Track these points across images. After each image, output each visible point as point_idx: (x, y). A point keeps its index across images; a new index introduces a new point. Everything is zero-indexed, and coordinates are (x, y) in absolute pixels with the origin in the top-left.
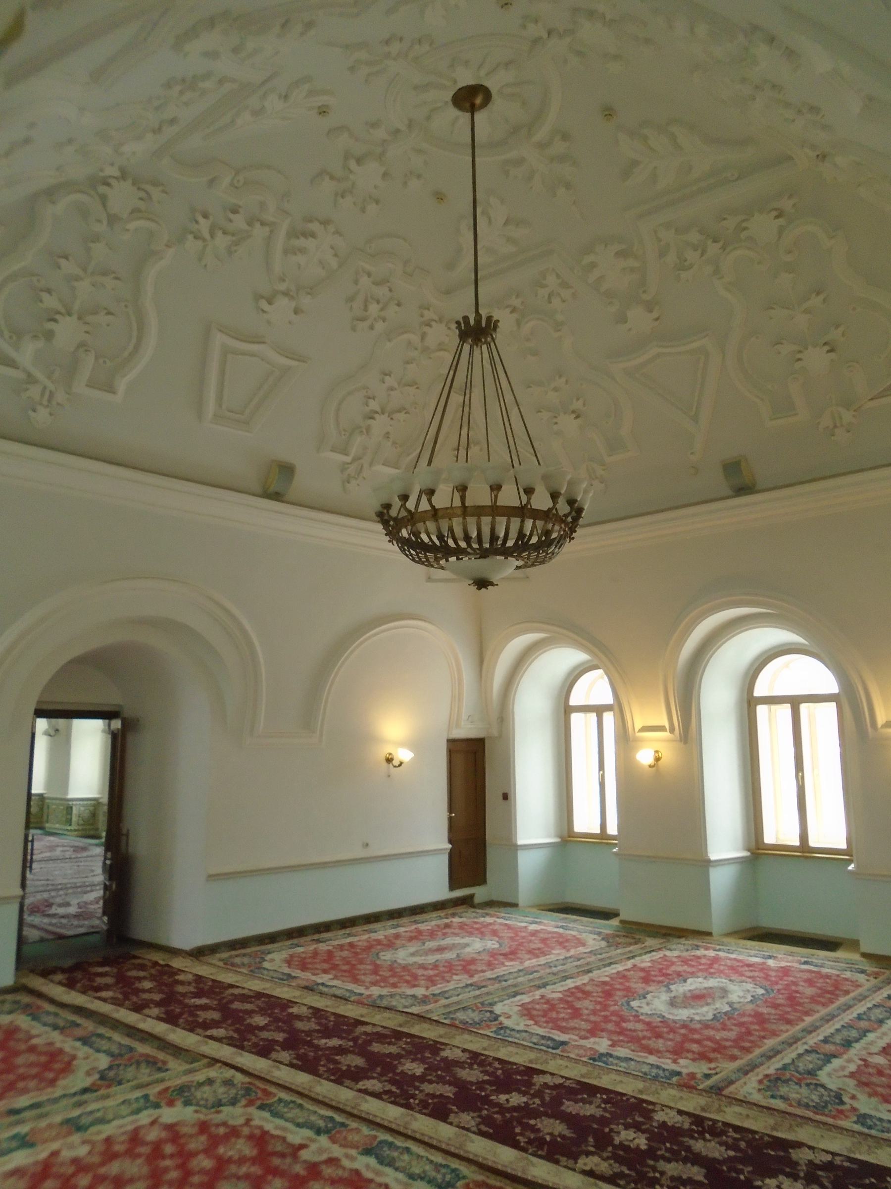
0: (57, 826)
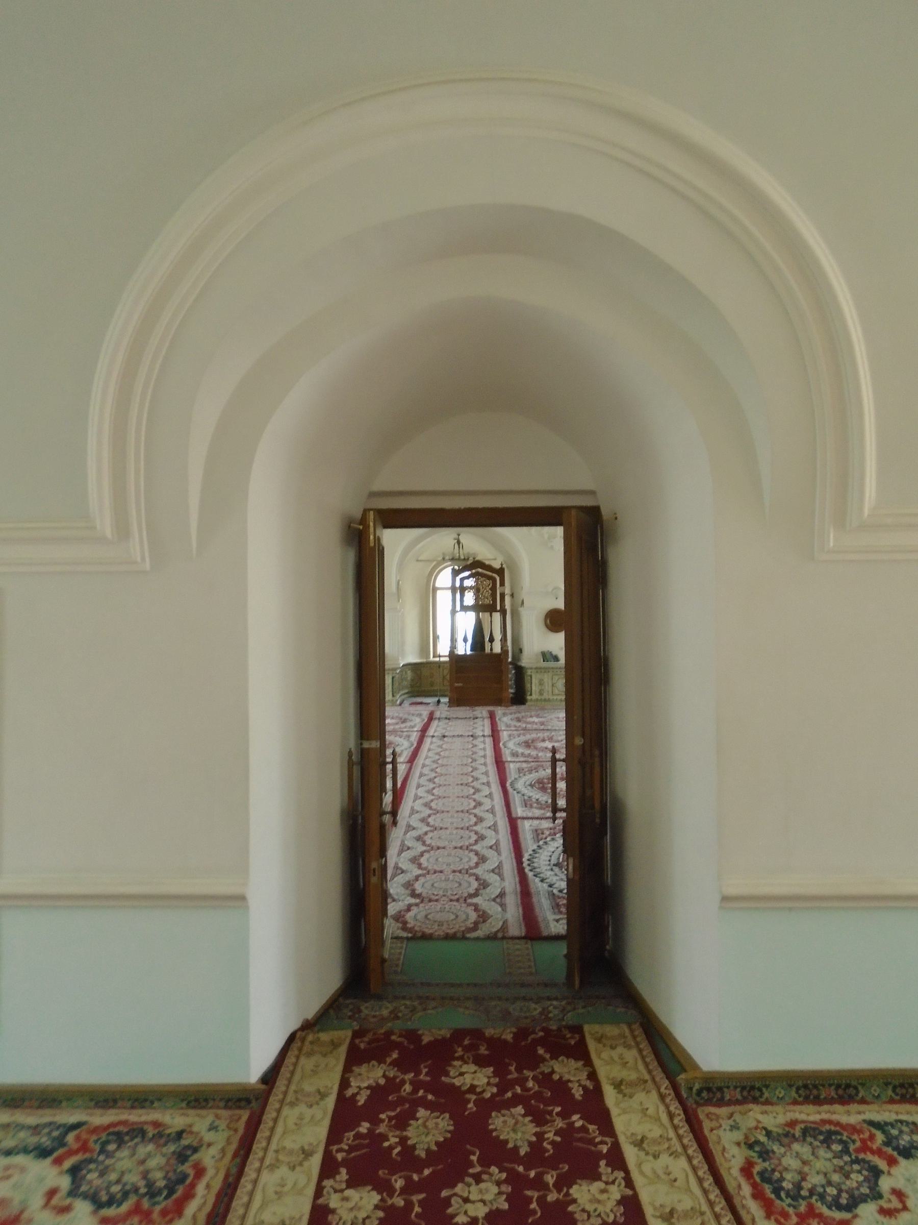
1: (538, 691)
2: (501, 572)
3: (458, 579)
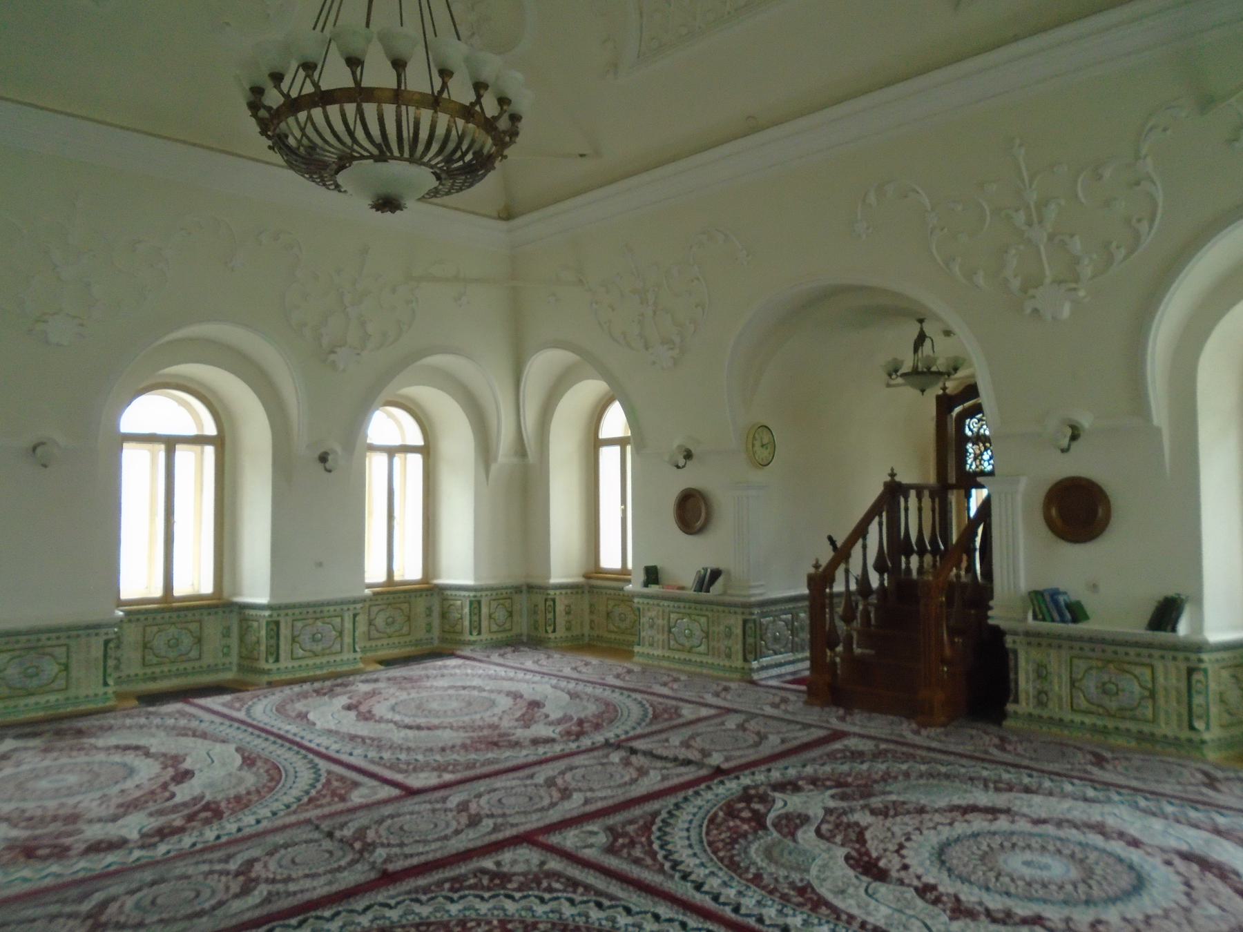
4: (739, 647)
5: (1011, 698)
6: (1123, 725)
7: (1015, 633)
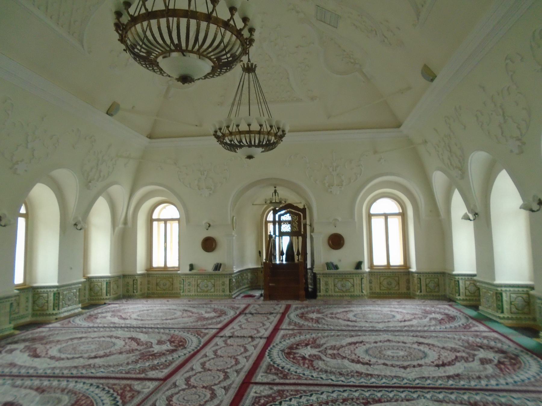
0: (490, 311)
1: (324, 289)
2: (304, 210)
3: (277, 216)
4: (228, 287)
5: (318, 291)
6: (347, 294)
7: (320, 274)
